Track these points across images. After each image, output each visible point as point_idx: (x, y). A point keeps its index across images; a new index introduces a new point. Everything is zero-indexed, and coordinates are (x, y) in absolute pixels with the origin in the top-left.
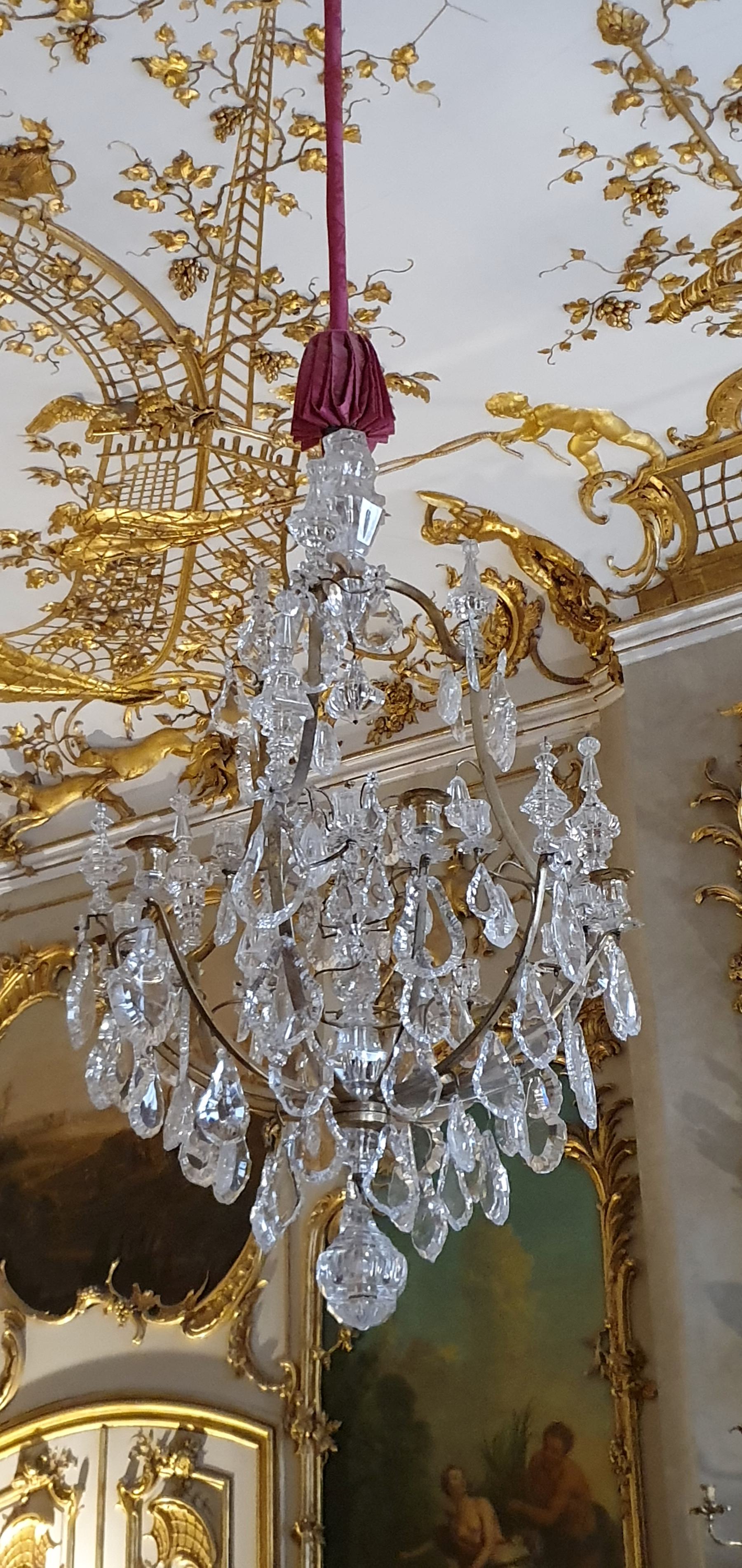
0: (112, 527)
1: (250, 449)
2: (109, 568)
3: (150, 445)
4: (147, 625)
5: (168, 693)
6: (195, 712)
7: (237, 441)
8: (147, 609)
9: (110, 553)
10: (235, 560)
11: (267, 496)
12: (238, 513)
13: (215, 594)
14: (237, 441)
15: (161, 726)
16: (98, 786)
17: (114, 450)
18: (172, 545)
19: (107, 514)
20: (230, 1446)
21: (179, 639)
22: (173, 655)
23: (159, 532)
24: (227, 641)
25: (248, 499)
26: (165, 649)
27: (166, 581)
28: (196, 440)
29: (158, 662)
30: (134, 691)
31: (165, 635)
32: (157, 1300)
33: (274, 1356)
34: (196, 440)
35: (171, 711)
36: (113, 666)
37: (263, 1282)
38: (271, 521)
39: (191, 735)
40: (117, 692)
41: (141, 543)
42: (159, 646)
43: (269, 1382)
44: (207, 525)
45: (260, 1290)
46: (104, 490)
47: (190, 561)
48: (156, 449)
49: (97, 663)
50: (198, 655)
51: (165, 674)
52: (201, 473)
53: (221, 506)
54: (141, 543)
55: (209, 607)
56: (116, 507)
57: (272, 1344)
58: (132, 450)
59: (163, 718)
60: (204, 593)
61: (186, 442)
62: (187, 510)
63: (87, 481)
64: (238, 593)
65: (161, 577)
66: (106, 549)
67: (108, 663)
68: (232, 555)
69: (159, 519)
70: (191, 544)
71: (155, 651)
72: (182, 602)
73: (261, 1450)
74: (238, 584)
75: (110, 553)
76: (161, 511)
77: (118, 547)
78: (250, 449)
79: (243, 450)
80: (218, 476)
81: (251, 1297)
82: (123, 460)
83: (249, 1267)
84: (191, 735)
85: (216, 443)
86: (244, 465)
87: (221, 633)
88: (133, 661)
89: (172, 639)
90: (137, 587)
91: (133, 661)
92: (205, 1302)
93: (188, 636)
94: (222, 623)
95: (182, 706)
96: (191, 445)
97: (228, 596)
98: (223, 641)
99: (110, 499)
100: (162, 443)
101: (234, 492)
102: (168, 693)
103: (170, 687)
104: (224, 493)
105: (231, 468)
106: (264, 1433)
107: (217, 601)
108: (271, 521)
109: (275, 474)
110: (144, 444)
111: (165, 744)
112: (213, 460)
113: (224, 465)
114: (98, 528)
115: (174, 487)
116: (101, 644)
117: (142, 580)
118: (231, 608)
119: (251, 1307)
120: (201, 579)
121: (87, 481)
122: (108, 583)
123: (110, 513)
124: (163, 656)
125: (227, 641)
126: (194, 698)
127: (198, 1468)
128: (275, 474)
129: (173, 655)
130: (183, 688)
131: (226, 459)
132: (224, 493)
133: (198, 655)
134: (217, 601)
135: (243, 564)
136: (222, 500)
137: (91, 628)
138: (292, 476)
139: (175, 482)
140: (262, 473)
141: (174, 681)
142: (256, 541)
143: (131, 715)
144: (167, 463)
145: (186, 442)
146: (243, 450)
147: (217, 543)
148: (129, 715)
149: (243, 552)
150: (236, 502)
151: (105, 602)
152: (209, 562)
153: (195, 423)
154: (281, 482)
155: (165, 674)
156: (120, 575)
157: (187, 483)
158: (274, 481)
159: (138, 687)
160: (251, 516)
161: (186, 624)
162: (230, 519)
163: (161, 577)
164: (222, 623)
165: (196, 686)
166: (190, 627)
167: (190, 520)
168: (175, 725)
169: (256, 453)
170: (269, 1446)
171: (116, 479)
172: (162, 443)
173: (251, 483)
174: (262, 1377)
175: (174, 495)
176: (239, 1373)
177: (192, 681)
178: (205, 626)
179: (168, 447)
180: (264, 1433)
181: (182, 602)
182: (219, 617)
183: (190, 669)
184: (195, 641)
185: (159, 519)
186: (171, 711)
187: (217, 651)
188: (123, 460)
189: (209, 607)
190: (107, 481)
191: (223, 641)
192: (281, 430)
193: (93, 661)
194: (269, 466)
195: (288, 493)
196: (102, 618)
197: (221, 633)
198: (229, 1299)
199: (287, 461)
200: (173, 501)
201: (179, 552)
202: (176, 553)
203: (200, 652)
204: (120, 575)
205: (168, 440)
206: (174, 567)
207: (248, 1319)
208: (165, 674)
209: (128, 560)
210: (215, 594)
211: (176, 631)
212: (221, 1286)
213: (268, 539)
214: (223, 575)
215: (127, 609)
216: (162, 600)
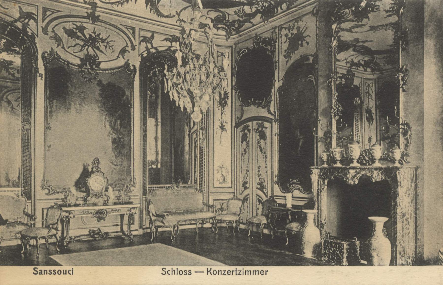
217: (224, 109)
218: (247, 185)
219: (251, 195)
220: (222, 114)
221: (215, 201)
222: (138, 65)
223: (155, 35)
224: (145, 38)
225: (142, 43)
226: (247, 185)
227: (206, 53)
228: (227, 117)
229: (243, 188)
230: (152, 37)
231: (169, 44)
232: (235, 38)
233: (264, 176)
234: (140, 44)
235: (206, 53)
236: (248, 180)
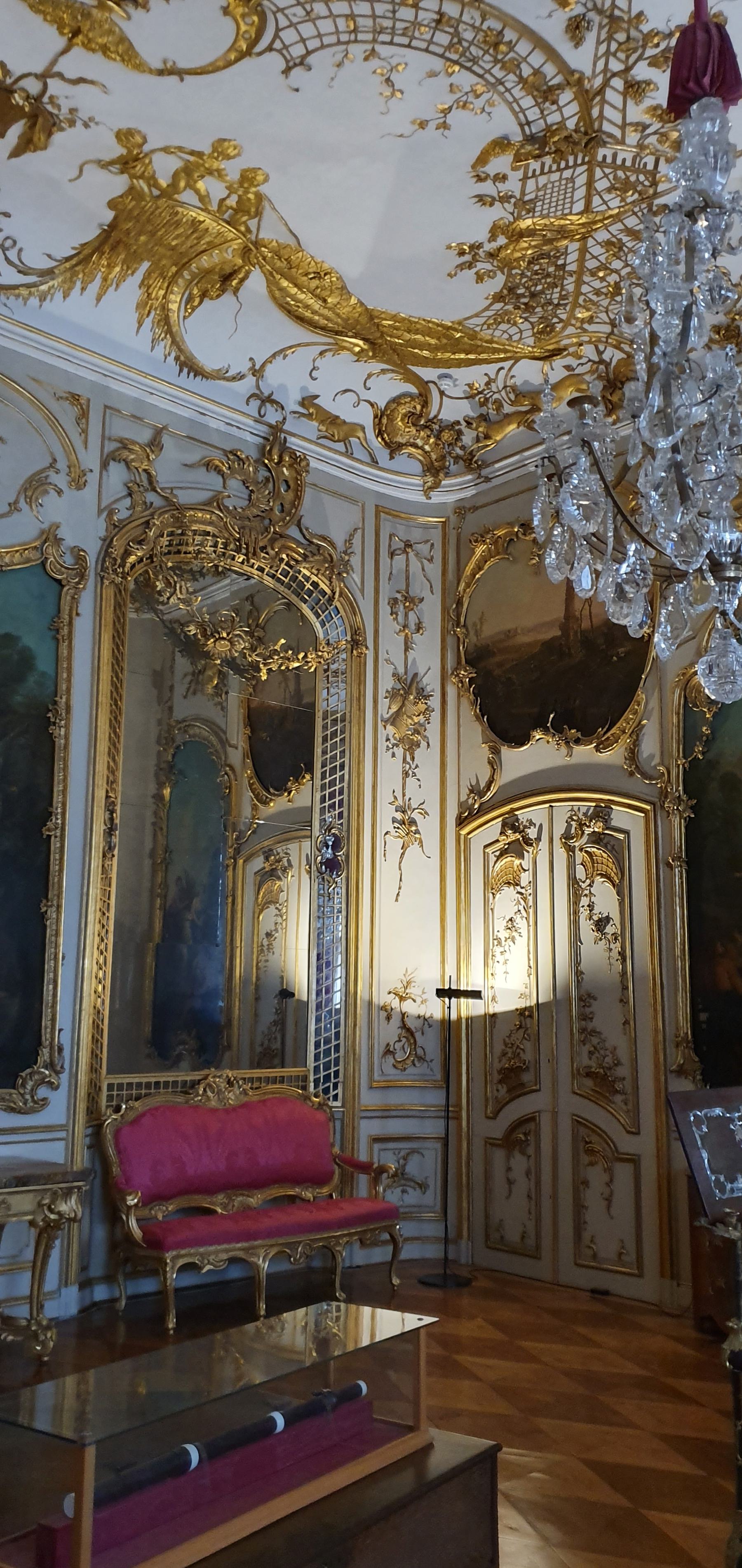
0: (531, 232)
1: (624, 160)
2: (530, 263)
3: (554, 167)
4: (556, 302)
5: (571, 350)
6: (590, 361)
7: (615, 156)
8: (556, 290)
9: (529, 252)
10: (615, 247)
11: (636, 196)
12: (617, 211)
13: (601, 274)
14: (615, 156)
15: (567, 373)
16: (526, 419)
17: (530, 175)
18: (572, 241)
19: (526, 223)
20: (626, 817)
21: (577, 310)
22: (573, 322)
23: (563, 233)
24: (611, 307)
25: (623, 200)
26: (569, 319)
27: (568, 268)
28: (587, 159)
29: (564, 328)
30: (549, 351)
31: (568, 308)
32: (579, 735)
33: (653, 764)
34: (587, 159)
35: (573, 362)
36: (534, 335)
37: (645, 722)
38: (640, 214)
39: (587, 378)
40: (537, 352)
41: (550, 241)
42: (564, 317)
43: (651, 779)
44: (595, 223)
45: (644, 726)
46: (525, 206)
47: (583, 251)
48: (558, 169)
49: (522, 333)
50: (590, 320)
51: (569, 337)
52: (590, 183)
53: (604, 207)
54: (550, 241)
55: (597, 284)
56: (533, 217)
57: (652, 757)
58: (542, 173)
59: (568, 368)
60: (593, 274)
61: (579, 161)
62: (581, 213)
63: (513, 200)
64: (617, 271)
65: (564, 265)
66: (527, 249)
67: (530, 333)
68: (613, 244)
69: (562, 222)
70: (584, 238)
71: (561, 321)
72: (579, 283)
73: (647, 818)
74: (617, 264)
75: (529, 252)
76: (564, 217)
77: (535, 247)
78: (624, 160)
79: (619, 162)
80: (602, 185)
81: (637, 731)
82: (537, 182)
83: (635, 713)
84: (587, 378)
85: (600, 158)
86: (620, 173)
87: (605, 303)
88: (547, 330)
89: (573, 310)
90: (548, 275)
91: (547, 330)
92: (609, 734)
93: (584, 307)
94: (606, 295)
95: (580, 357)
96: (583, 163)
97: (610, 274)
98: (607, 308)
99: (528, 212)
100: (563, 165)
101: (613, 195)
102: (571, 350)
103: (573, 345)
104: (606, 197)
105: (611, 177)
106: (648, 807)
107: (602, 279)
108: (640, 214)
109: (642, 178)
110: (550, 167)
111: (569, 386)
112: (598, 173)
113: (606, 176)
114: (522, 234)
115: (572, 197)
116: (526, 319)
117: (551, 269)
118: (612, 283)
119: (638, 736)
120: (591, 264)
121: (513, 200)
122: (529, 274)
123: (529, 222)
124: (567, 324)
125: (611, 307)
126: (588, 351)
127: (607, 829)
128: (642, 178)
129: (573, 322)
130: (581, 345)
131: (607, 171)
132: (606, 197)
133: (590, 320)
134: (602, 279)
135: (620, 249)
136: (605, 202)
137: (519, 308)
138: (654, 177)
139: (572, 192)
140: (633, 179)
141: (575, 340)
142: (629, 232)
143: (547, 368)
144: (567, 179)
145: (579, 161)
146: (619, 162)
147: (602, 236)
148: (545, 368)
149: (620, 240)
150: (615, 203)
151: (527, 288)
152: (597, 250)
153: (586, 146)
154: (647, 183)
155: (569, 337)
156: (537, 267)
157: (581, 193)
158: (642, 183)
159: (551, 347)
160: (625, 212)
161: (581, 298)
162: (611, 216)
163: (564, 265)
164: (606, 295)
165: (590, 342)
166: (585, 300)
167: (583, 220)
168: (576, 372)
169: (628, 163)
170: (652, 815)
171: (533, 196)
172: (563, 165)
173: (624, 187)
174: (645, 775)
175: (572, 203)
176: (631, 774)
177: (587, 339)
178: (594, 298)
179: (567, 167)
180: (648, 807)
181: (579, 283)
182: (604, 290)
183: (585, 331)
184: (588, 310)
185: (562, 222)
186: (573, 362)
187: (603, 316)
188: (537, 182)
189: (597, 284)
190: (527, 198)
191: (607, 308)
192: (646, 142)
193: (521, 332)
194: (638, 171)
195: (651, 191)
196: (525, 300)
197: (605, 303)
198: (624, 732)
199: (650, 167)
200: (571, 208)
201: (575, 246)
202: (574, 246)
203: (591, 317)
204: (537, 267)
205: (567, 162)
206: (573, 257)
207: (636, 743)
208: (568, 336)
209: (542, 256)
210: (601, 274)
211: (576, 304)
212: (618, 725)
213: (637, 228)
214: (607, 258)
215: (542, 292)
216: (565, 282)
217: (413, 759)
218: (527, 1077)
219: (545, 1122)
220: (406, 774)
221: (377, 1146)
222: (92, 550)
223: (166, 439)
224: (124, 444)
225: (113, 466)
226: (527, 1077)
227: (352, 536)
228: (425, 790)
229: (503, 1090)
230: (155, 444)
231: (216, 481)
232: (456, 489)
233: (615, 1038)
234: (104, 465)
235: (352, 536)
236: (528, 1056)
